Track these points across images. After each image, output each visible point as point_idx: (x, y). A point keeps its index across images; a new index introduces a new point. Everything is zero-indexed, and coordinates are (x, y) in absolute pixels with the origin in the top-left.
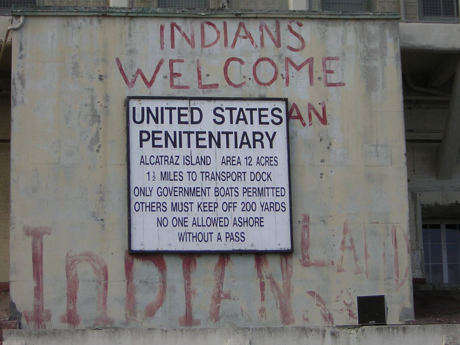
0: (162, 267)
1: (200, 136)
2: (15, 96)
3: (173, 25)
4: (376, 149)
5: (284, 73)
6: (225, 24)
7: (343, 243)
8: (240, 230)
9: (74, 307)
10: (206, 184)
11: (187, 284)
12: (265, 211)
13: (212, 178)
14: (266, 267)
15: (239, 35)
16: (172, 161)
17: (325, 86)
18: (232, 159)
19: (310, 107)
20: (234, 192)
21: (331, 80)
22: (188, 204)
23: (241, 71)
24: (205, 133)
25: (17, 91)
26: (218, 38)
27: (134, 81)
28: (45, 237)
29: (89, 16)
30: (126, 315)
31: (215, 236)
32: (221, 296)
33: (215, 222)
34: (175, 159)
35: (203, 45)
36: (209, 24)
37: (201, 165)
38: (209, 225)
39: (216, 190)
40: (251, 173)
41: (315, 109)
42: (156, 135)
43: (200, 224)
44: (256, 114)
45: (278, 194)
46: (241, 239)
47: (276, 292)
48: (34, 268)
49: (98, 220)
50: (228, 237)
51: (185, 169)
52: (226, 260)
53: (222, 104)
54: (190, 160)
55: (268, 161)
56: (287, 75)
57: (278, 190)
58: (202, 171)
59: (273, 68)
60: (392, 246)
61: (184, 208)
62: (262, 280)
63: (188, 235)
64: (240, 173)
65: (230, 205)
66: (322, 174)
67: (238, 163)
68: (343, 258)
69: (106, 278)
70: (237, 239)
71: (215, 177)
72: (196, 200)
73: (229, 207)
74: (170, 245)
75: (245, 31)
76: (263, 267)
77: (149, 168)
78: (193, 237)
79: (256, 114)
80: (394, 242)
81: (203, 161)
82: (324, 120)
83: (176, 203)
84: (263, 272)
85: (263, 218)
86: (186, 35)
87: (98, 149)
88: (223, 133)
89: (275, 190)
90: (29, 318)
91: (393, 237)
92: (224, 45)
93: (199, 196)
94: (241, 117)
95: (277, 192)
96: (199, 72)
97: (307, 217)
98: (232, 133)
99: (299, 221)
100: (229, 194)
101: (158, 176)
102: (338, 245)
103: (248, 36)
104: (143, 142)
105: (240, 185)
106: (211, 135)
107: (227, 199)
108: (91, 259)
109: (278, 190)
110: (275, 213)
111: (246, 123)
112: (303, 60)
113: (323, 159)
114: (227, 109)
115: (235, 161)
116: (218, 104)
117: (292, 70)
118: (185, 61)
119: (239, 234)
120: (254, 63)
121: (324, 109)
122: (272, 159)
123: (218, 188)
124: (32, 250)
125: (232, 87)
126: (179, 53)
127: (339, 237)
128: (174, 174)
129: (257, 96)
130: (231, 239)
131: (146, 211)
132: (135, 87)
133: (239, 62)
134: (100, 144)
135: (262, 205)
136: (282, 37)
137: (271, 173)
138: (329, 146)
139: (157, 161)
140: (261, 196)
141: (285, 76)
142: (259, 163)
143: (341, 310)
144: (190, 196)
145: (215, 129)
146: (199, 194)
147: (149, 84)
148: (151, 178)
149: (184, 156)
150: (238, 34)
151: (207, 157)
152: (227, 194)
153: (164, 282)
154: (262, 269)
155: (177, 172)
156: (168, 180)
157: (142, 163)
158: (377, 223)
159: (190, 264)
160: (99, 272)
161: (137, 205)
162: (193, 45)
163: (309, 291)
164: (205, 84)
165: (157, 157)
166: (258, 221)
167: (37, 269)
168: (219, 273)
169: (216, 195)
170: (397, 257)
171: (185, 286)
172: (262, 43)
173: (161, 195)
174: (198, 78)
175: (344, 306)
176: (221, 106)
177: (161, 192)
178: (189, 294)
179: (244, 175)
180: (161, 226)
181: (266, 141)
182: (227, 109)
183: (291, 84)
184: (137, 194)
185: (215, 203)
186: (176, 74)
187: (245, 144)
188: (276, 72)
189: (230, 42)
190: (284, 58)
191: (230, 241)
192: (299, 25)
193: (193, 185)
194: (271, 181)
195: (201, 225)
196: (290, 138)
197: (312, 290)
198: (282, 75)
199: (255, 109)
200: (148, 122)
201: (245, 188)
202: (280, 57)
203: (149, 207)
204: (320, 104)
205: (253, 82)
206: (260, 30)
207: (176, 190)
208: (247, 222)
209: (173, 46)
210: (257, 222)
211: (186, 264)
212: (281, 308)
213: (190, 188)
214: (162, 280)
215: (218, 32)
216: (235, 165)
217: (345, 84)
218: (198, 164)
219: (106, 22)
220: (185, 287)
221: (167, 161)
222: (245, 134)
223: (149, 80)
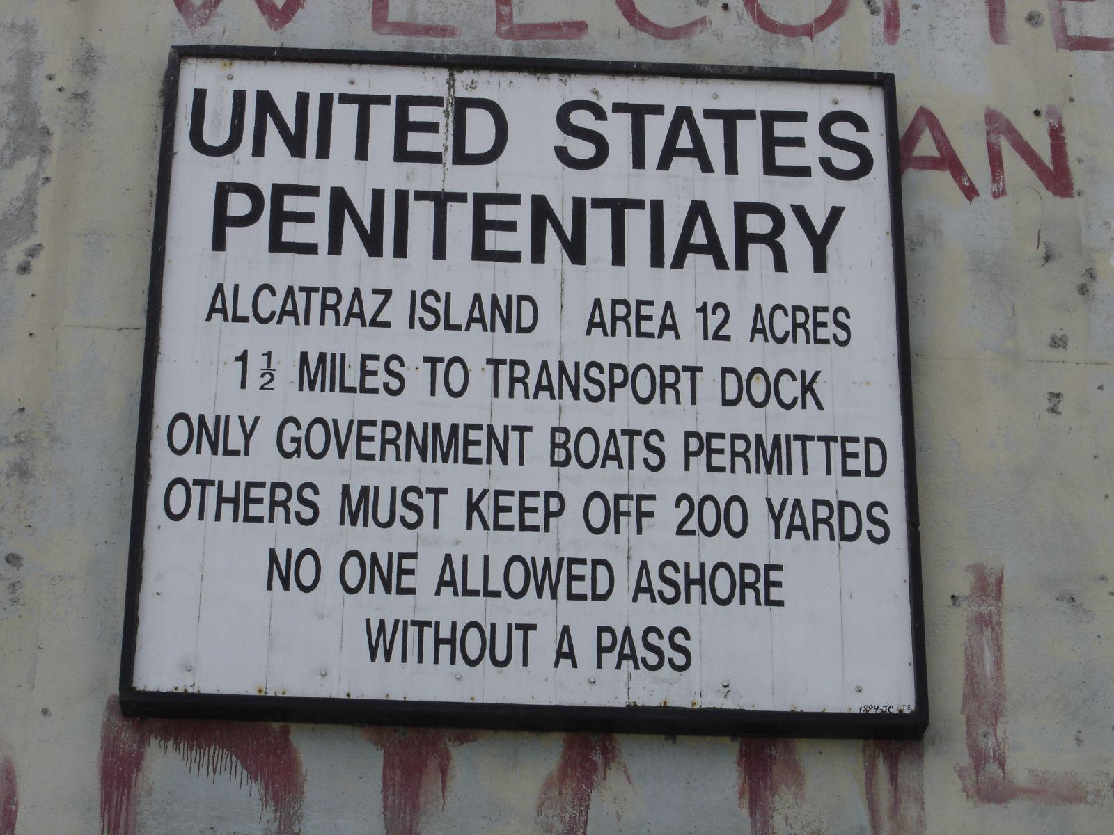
1: (493, 212)
8: (666, 617)
12: (788, 536)
13: (539, 388)
16: (356, 309)
17: (1057, 47)
18: (638, 310)
19: (995, 122)
22: (421, 496)
24: (514, 200)
31: (544, 643)
34: (371, 304)
37: (489, 333)
39: (557, 441)
40: (725, 371)
41: (1019, 136)
42: (291, 203)
43: (475, 583)
44: (749, 135)
45: (852, 464)
46: (671, 660)
50: (610, 649)
52: (598, 758)
53: (598, 88)
54: (440, 307)
55: (803, 326)
57: (850, 447)
61: (400, 510)
63: (413, 632)
64: (673, 369)
65: (623, 505)
66: (1058, 395)
67: (664, 327)
70: (653, 659)
73: (619, 514)
74: (324, 675)
78: (438, 642)
79: (749, 135)
81: (501, 315)
83: (364, 491)
85: (779, 568)
87: (28, 263)
88: (598, 203)
93: (477, 461)
94: (685, 141)
95: (846, 455)
97: (993, 579)
98: (639, 204)
99: (953, 597)
100: (617, 458)
101: (287, 370)
104: (231, 232)
106: (541, 209)
107: (610, 480)
109: (850, 447)
111: (707, 167)
113: (1059, 336)
114: (618, 108)
115: (649, 318)
116: (579, 88)
119: (661, 637)
121: (1056, 135)
122: (821, 317)
123: (565, 431)
125: (645, 36)
128: (363, 365)
130: (622, 657)
131: (218, 518)
135: (777, 509)
137: (817, 374)
138: (1083, 281)
139: (289, 307)
140: (769, 471)
142: (763, 331)
144: (434, 460)
146: (474, 452)
148: (254, 379)
149: (413, 294)
151: (521, 298)
152: (607, 457)
155: (376, 358)
156: (332, 389)
159: (420, 772)
161: (179, 490)
165: (290, 291)
166: (757, 580)
168: (562, 819)
169: (556, 459)
176: (592, 98)
177: (294, 440)
181: (794, 241)
182: (618, 108)
184: (180, 443)
185: (549, 495)
191: (618, 667)
193: (447, 413)
194: (820, 407)
195: (480, 587)
196: (907, 242)
199: (749, 115)
200: (258, 150)
201: (696, 435)
204: (1037, 113)
205: (740, 19)
207: (367, 431)
208: (701, 582)
210: (753, 586)
211: (398, 772)
213: (437, 427)
216: (651, 335)
218: (476, 327)
221: (334, 308)
222: (699, 210)
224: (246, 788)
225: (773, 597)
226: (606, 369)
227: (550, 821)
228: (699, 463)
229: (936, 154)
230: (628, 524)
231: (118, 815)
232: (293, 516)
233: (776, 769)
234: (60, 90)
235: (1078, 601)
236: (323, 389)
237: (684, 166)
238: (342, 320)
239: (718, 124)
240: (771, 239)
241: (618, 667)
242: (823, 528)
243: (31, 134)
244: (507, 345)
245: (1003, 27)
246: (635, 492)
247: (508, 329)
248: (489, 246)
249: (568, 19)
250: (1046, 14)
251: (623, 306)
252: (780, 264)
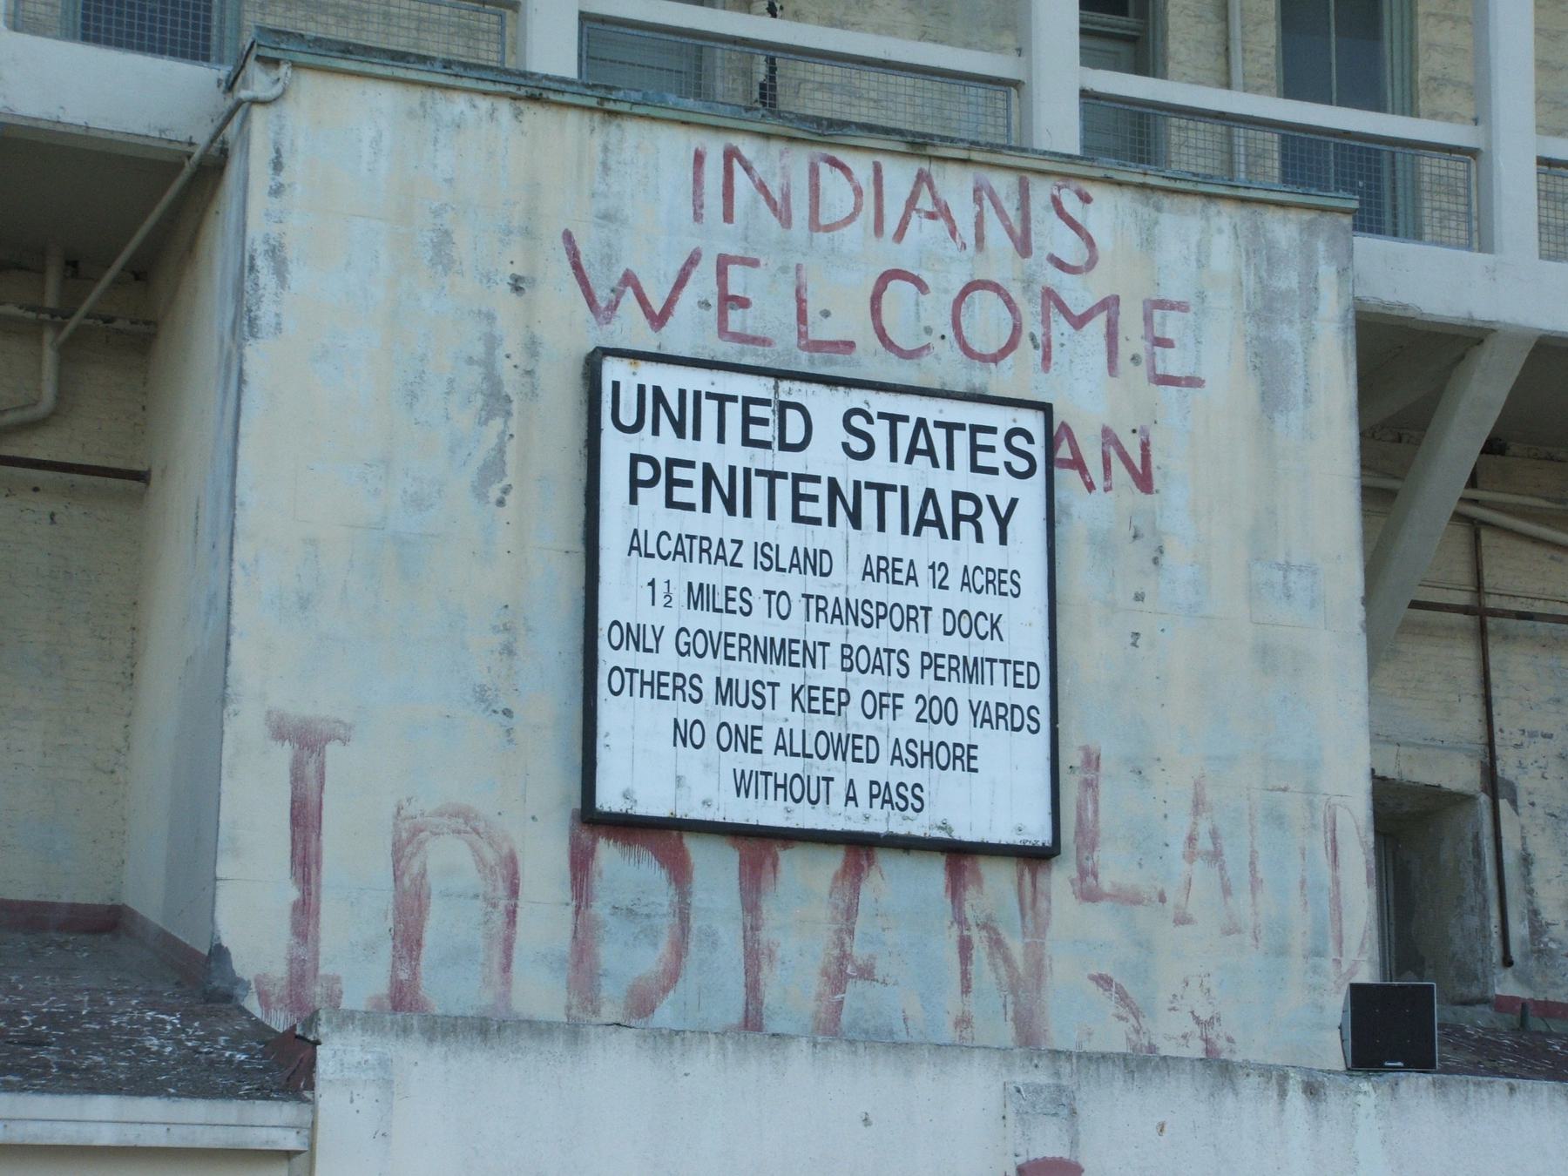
0: (679, 870)
1: (805, 488)
2: (254, 308)
3: (730, 154)
4: (1285, 577)
5: (1039, 332)
6: (877, 169)
7: (1191, 839)
8: (911, 776)
9: (414, 974)
10: (818, 631)
11: (752, 928)
12: (981, 727)
13: (834, 616)
14: (978, 892)
15: (917, 207)
16: (721, 554)
18: (893, 565)
19: (1108, 436)
20: (895, 665)
21: (1165, 368)
23: (918, 313)
24: (816, 479)
25: (261, 292)
26: (857, 208)
27: (613, 306)
28: (332, 749)
29: (485, 93)
30: (569, 1008)
31: (838, 788)
32: (848, 971)
33: (842, 747)
34: (730, 549)
35: (814, 224)
36: (834, 163)
38: (822, 754)
41: (1123, 448)
42: (679, 473)
43: (798, 748)
44: (962, 440)
45: (1021, 680)
47: (1003, 971)
48: (293, 840)
49: (495, 712)
50: (877, 796)
51: (759, 581)
52: (864, 863)
55: (992, 582)
56: (1044, 338)
58: (808, 593)
59: (1006, 314)
60: (1323, 859)
61: (752, 696)
62: (966, 933)
63: (761, 778)
64: (914, 607)
66: (1137, 634)
67: (909, 578)
69: (514, 891)
70: (902, 804)
71: (846, 612)
72: (788, 677)
75: (934, 197)
76: (967, 893)
77: (655, 568)
78: (777, 786)
79: (962, 440)
80: (1329, 848)
82: (1144, 481)
83: (730, 681)
85: (975, 747)
86: (768, 188)
88: (869, 485)
89: (1010, 667)
90: (273, 999)
91: (1329, 834)
92: (873, 233)
93: (797, 665)
94: (922, 444)
95: (1016, 673)
96: (801, 301)
97: (1094, 757)
98: (893, 488)
100: (880, 667)
101: (680, 595)
102: (1178, 847)
103: (941, 212)
104: (641, 491)
105: (914, 643)
106: (833, 486)
107: (876, 682)
108: (468, 829)
111: (935, 464)
112: (1091, 301)
114: (882, 416)
115: (900, 571)
116: (857, 398)
117: (1060, 325)
118: (762, 262)
120: (955, 293)
121: (1145, 447)
122: (1004, 577)
123: (850, 647)
124: (288, 788)
125: (892, 355)
126: (746, 239)
127: (1180, 824)
129: (960, 388)
130: (884, 801)
132: (616, 324)
133: (913, 285)
134: (506, 482)
136: (1034, 226)
137: (1000, 616)
139: (679, 549)
140: (971, 682)
141: (1039, 339)
142: (968, 584)
143: (1184, 1037)
145: (848, 473)
146: (796, 659)
147: (658, 320)
148: (660, 600)
150: (915, 204)
151: (823, 551)
152: (875, 667)
153: (683, 914)
155: (734, 589)
156: (708, 610)
158: (1285, 790)
160: (493, 872)
161: (616, 675)
162: (786, 221)
163: (1095, 973)
164: (817, 338)
165: (680, 536)
167: (305, 846)
170: (1339, 894)
171: (745, 932)
172: (980, 239)
173: (688, 652)
174: (798, 319)
175: (1191, 1026)
176: (864, 407)
178: (754, 958)
180: (685, 745)
181: (988, 520)
182: (882, 416)
185: (841, 690)
186: (735, 298)
187: (930, 523)
189: (891, 225)
190: (1038, 289)
191: (882, 808)
192: (1081, 198)
193: (779, 631)
194: (1001, 639)
195: (800, 751)
197: (1106, 970)
198: (1033, 338)
200: (656, 431)
202: (1028, 283)
203: (651, 684)
204: (1134, 431)
205: (952, 347)
206: (974, 199)
207: (730, 640)
209: (728, 216)
210: (960, 758)
212: (1015, 1020)
213: (772, 640)
214: (677, 911)
215: (858, 192)
216: (900, 583)
217: (1204, 381)
218: (795, 570)
219: (536, 116)
220: (744, 937)
221: (707, 551)
222: (930, 495)
223: (657, 307)
224: (658, 873)
225: (972, 767)
226: (874, 605)
228: (929, 673)
229: (1071, 458)
230: (888, 712)
231: (582, 888)
232: (687, 697)
233: (966, 874)
234: (515, 366)
235: (1143, 774)
236: (702, 609)
237: (921, 461)
238: (713, 561)
239: (943, 432)
240: (973, 519)
241: (882, 808)
242: (1001, 722)
243: (498, 400)
244: (814, 585)
246: (891, 692)
247: (815, 574)
248: (802, 513)
249: (843, 339)
250: (1143, 355)
252: (979, 538)
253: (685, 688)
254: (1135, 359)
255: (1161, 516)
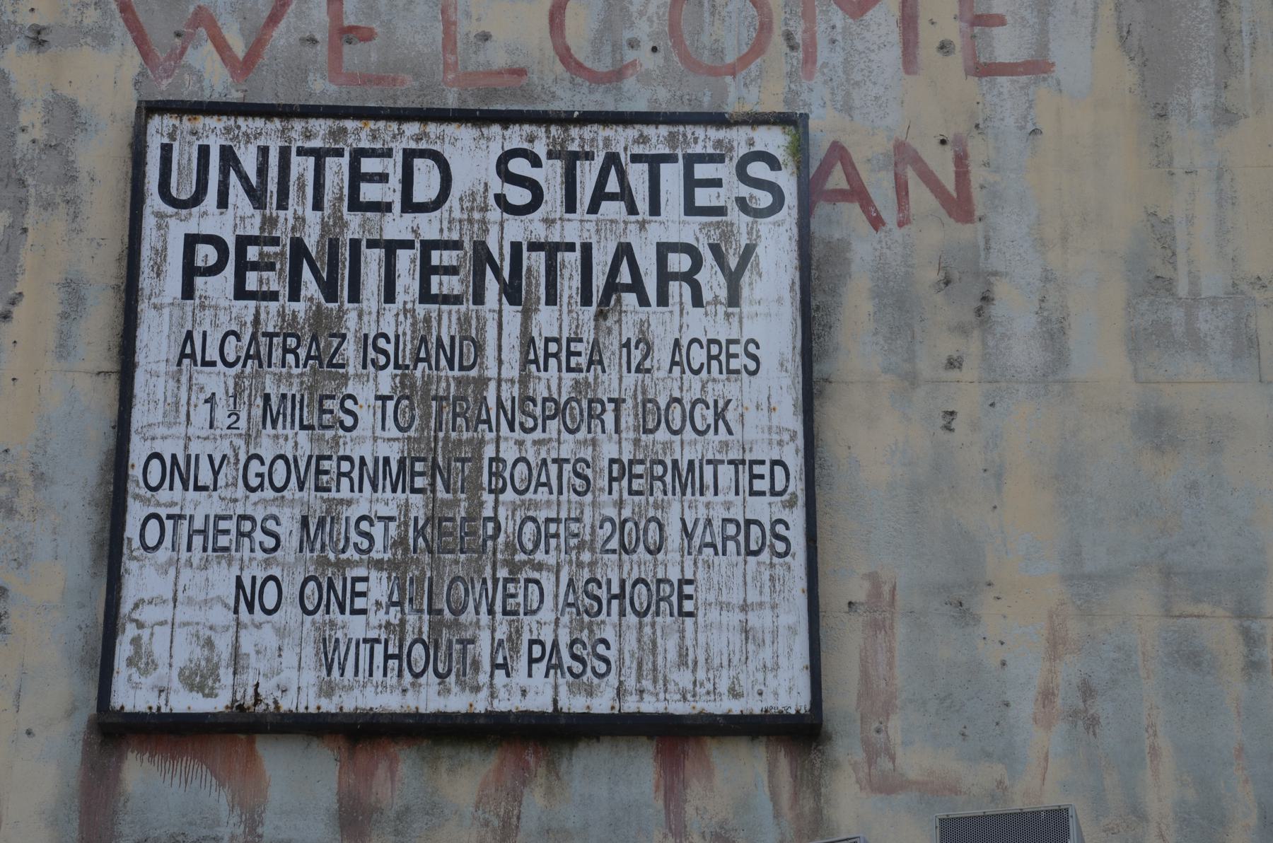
7: (1047, 696)
12: (700, 552)
17: (966, 75)
19: (903, 155)
22: (372, 525)
24: (456, 245)
44: (671, 176)
45: (759, 485)
54: (390, 348)
55: (717, 358)
57: (757, 470)
61: (354, 537)
65: (553, 528)
66: (952, 413)
67: (591, 362)
68: (1046, 760)
70: (577, 667)
76: (688, 791)
78: (387, 657)
79: (671, 176)
84: (690, 810)
85: (690, 582)
94: (613, 186)
95: (753, 477)
96: (449, 25)
97: (886, 589)
98: (570, 247)
99: (850, 603)
102: (1025, 707)
104: (199, 281)
109: (757, 470)
110: (746, 562)
113: (955, 357)
114: (551, 155)
116: (515, 137)
121: (961, 161)
122: (734, 349)
123: (504, 461)
138: (980, 304)
152: (539, 484)
154: (685, 801)
157: (186, 361)
161: (153, 525)
168: (498, 815)
173: (261, 485)
174: (444, 47)
177: (258, 475)
179: (617, 411)
181: (712, 280)
183: (826, 71)
184: (154, 480)
186: (352, 29)
188: (762, 25)
194: (730, 432)
198: (788, 36)
200: (223, 202)
203: (204, 532)
205: (666, 59)
213: (387, 461)
217: (1053, 64)
222: (625, 251)
223: (239, 48)
227: (487, 816)
232: (257, 547)
237: (611, 209)
240: (689, 277)
241: (547, 675)
242: (731, 545)
245: (915, 57)
248: (434, 290)
250: (958, 42)
251: (555, 344)
253: (254, 535)
254: (944, 47)
255: (988, 249)
